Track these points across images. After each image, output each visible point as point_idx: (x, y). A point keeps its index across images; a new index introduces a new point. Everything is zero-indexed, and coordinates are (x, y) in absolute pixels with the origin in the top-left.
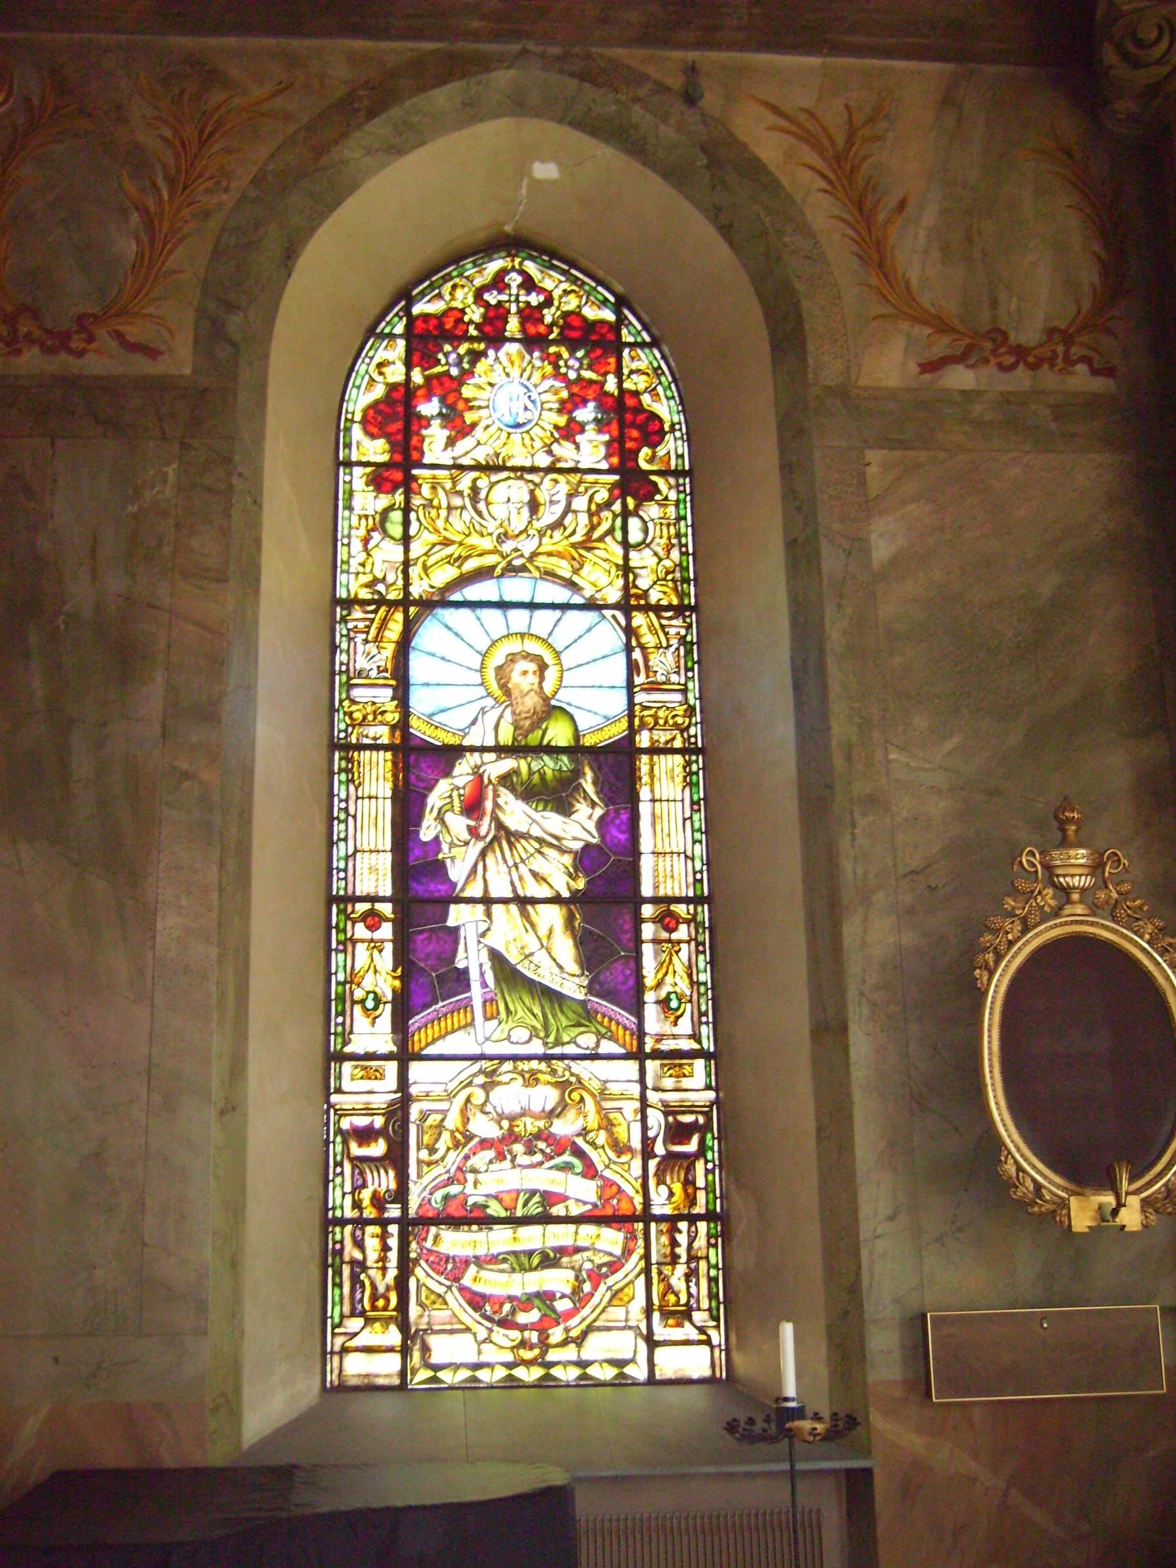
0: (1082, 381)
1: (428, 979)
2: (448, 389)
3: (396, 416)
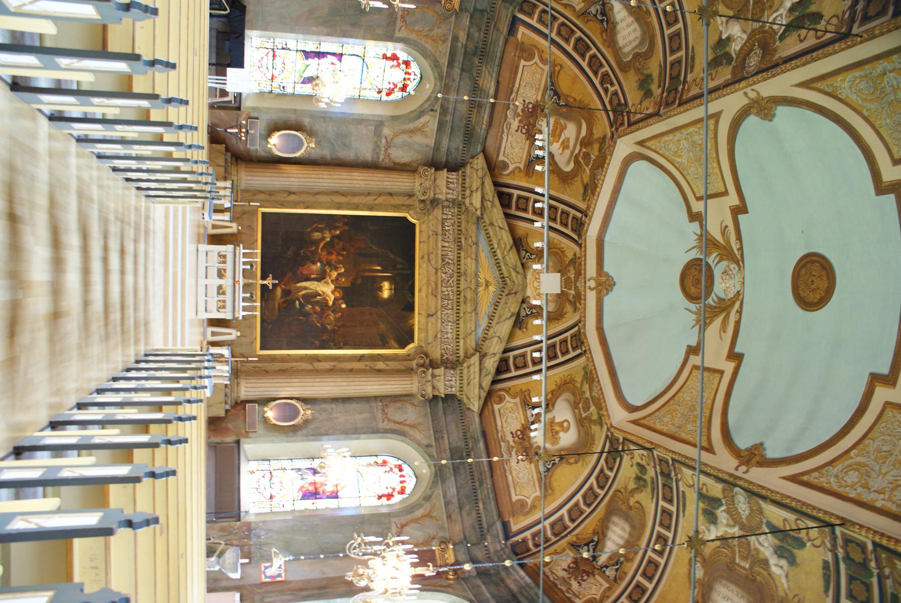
0: (382, 157)
1: (307, 55)
2: (399, 65)
3: (394, 57)
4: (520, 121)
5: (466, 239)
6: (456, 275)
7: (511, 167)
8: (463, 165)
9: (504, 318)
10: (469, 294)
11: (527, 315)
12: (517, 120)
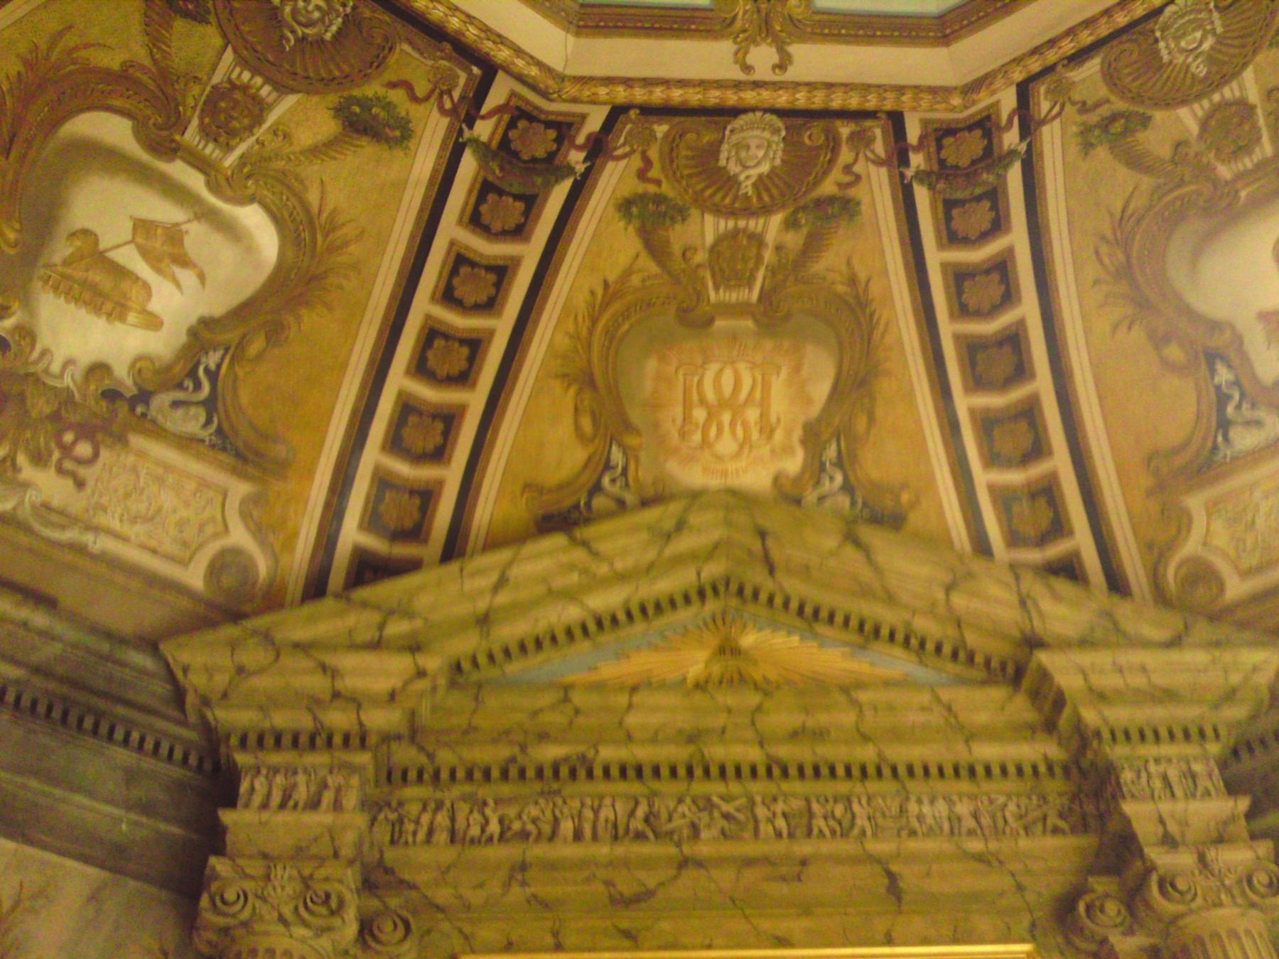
4: (39, 459)
5: (543, 737)
6: (700, 787)
7: (240, 536)
8: (213, 738)
9: (866, 574)
10: (781, 718)
11: (848, 488)
12: (28, 472)
